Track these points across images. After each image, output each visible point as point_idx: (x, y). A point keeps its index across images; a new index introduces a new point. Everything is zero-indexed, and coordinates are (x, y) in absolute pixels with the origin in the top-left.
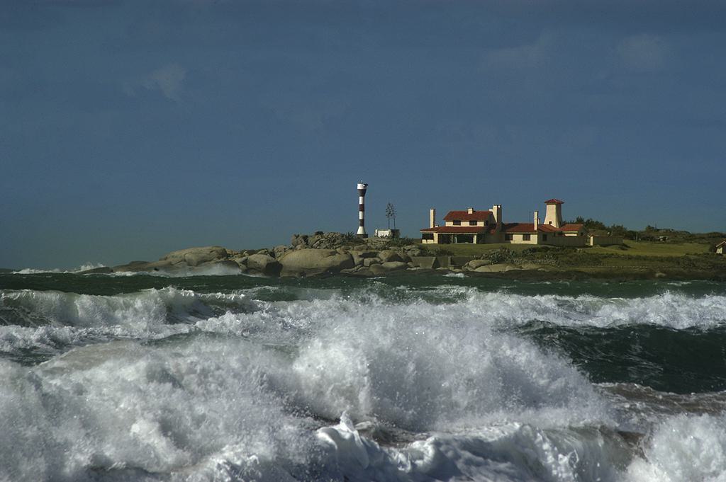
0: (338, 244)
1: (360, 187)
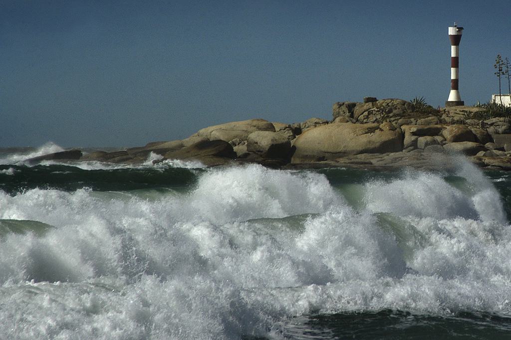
0: (395, 115)
1: (452, 31)
